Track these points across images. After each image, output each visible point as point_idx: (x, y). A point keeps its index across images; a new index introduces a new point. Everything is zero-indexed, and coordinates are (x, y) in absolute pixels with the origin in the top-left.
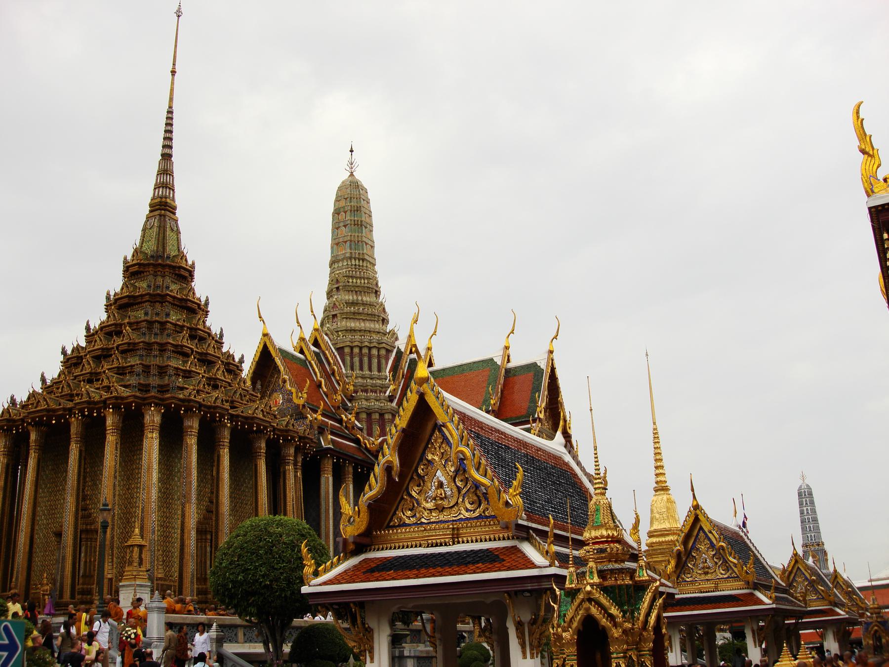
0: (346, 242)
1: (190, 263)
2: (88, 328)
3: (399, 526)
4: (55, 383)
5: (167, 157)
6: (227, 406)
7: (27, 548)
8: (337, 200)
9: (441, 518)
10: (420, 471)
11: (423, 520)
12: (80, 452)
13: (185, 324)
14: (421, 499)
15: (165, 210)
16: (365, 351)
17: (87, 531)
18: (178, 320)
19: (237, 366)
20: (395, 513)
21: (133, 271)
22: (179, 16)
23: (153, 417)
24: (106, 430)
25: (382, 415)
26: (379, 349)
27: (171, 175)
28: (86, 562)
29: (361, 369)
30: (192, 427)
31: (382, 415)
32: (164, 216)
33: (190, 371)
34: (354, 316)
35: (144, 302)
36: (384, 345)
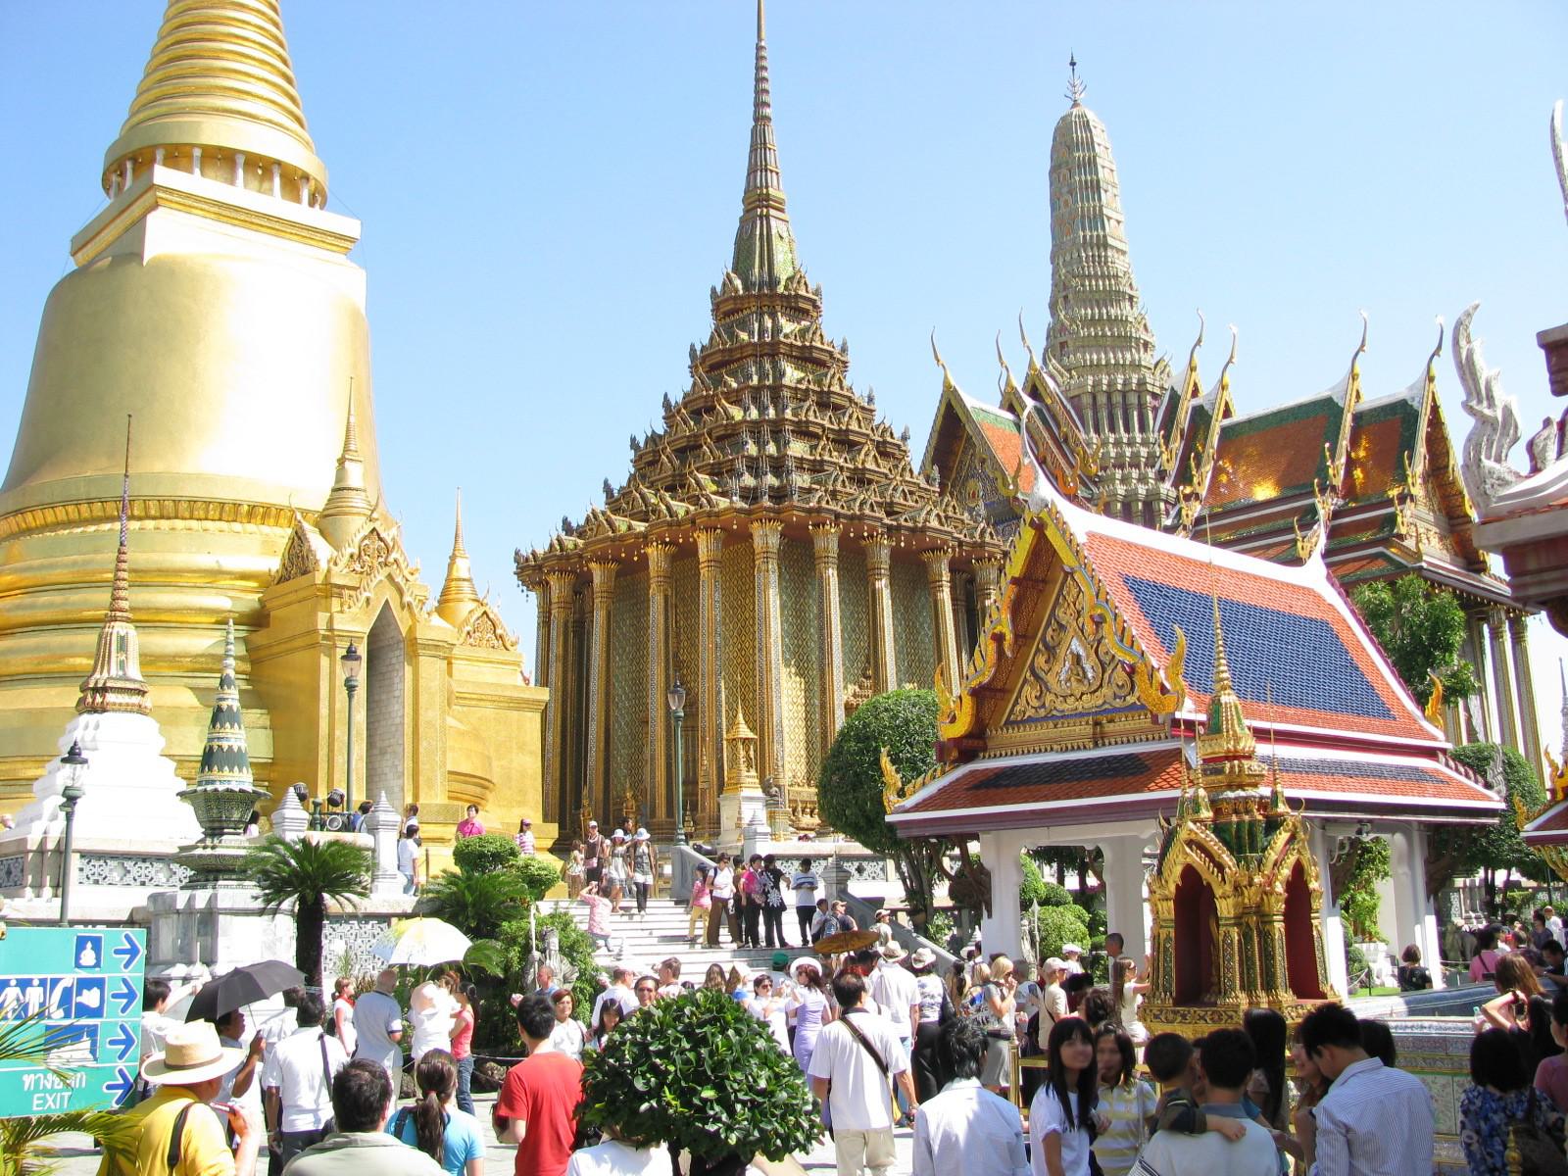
1: (812, 287)
2: (667, 404)
3: (1023, 722)
4: (624, 495)
5: (760, 120)
6: (881, 514)
7: (602, 745)
8: (1054, 149)
9: (1080, 709)
10: (1048, 638)
11: (1054, 713)
12: (666, 598)
13: (812, 387)
14: (1050, 679)
15: (767, 207)
18: (799, 381)
19: (899, 446)
20: (1016, 703)
21: (728, 309)
29: (1113, 429)
30: (826, 550)
32: (768, 217)
33: (822, 461)
34: (1097, 343)
35: (745, 357)
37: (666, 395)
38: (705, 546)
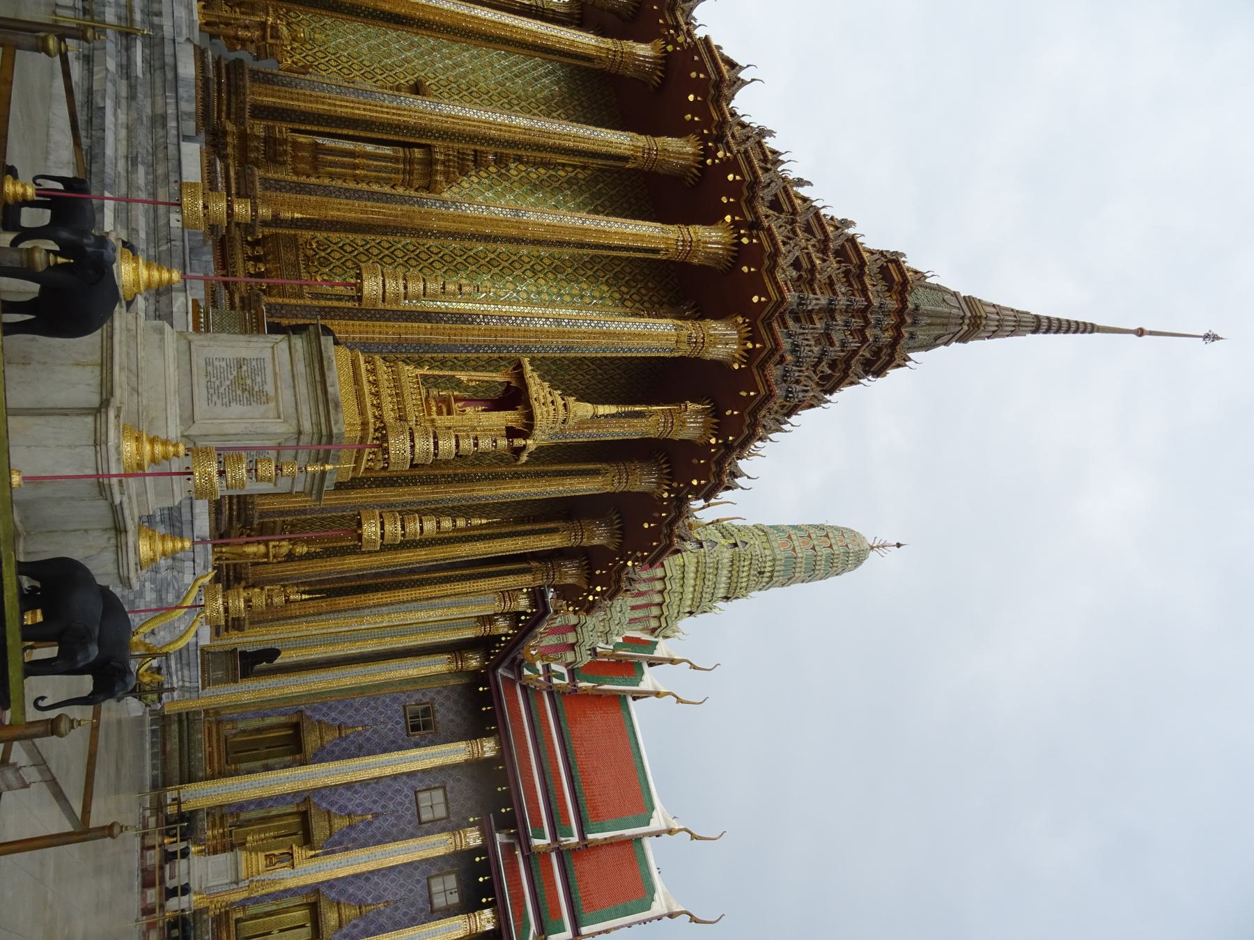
0: (794, 550)
12: (624, 159)
16: (657, 599)
17: (429, 163)
22: (1206, 337)
23: (722, 339)
24: (688, 221)
25: (572, 647)
26: (658, 617)
27: (1013, 333)
28: (352, 154)
31: (572, 647)
36: (664, 625)
37: (809, 183)
38: (711, 238)
